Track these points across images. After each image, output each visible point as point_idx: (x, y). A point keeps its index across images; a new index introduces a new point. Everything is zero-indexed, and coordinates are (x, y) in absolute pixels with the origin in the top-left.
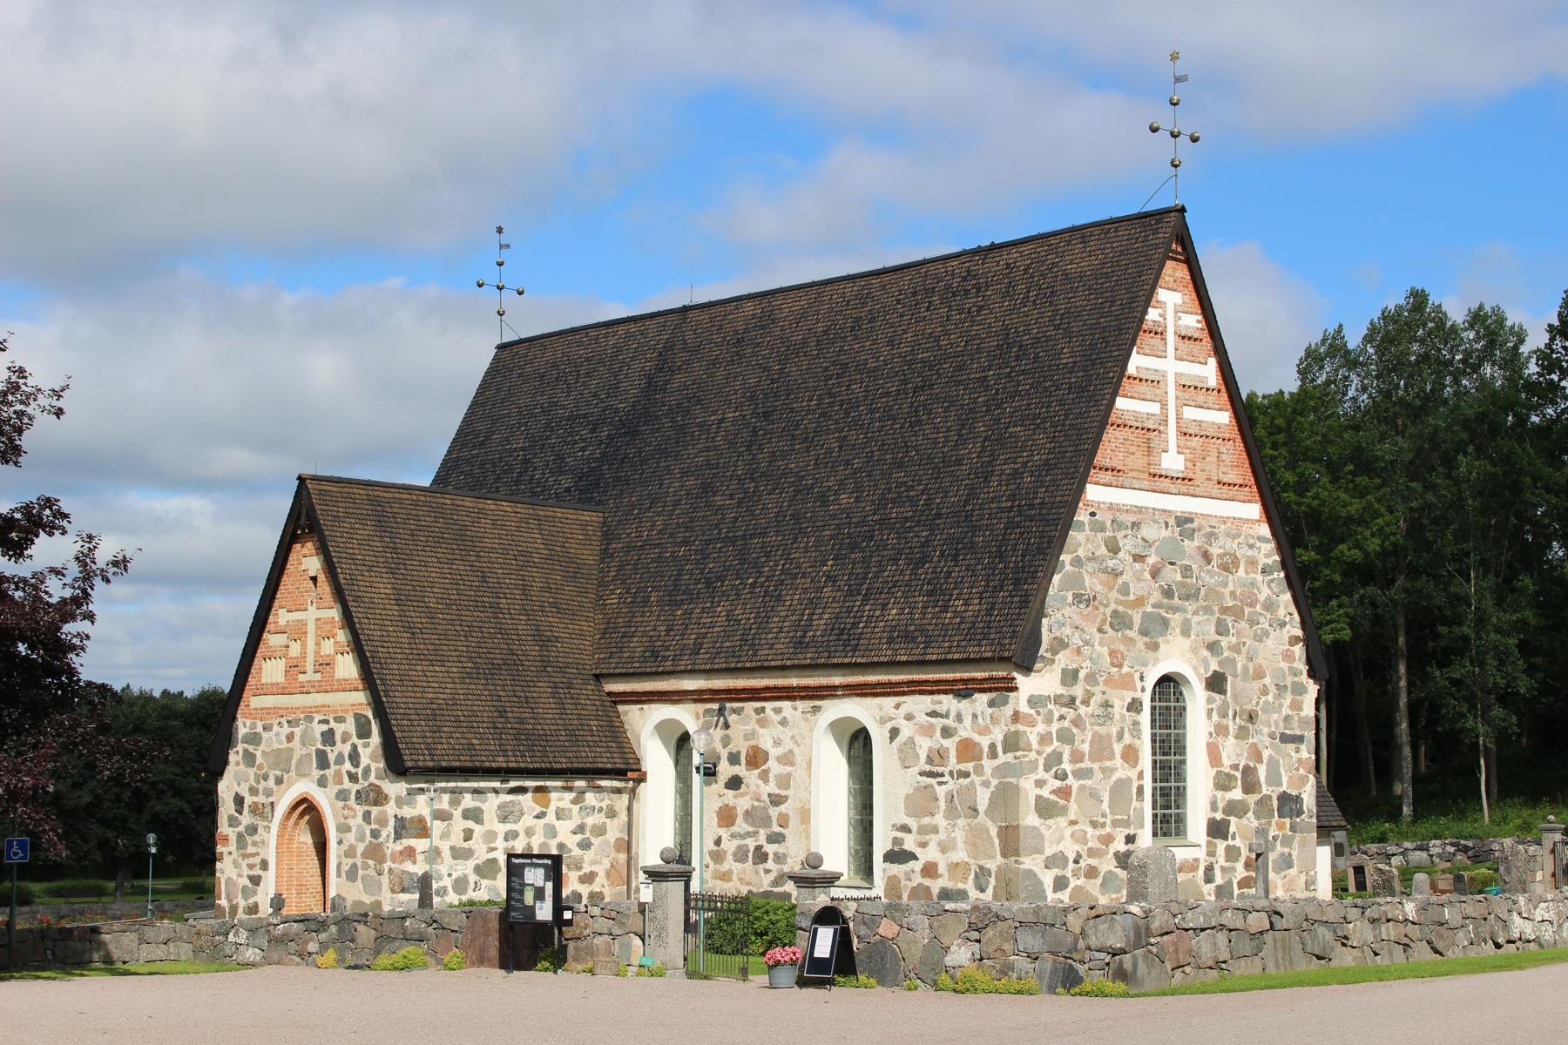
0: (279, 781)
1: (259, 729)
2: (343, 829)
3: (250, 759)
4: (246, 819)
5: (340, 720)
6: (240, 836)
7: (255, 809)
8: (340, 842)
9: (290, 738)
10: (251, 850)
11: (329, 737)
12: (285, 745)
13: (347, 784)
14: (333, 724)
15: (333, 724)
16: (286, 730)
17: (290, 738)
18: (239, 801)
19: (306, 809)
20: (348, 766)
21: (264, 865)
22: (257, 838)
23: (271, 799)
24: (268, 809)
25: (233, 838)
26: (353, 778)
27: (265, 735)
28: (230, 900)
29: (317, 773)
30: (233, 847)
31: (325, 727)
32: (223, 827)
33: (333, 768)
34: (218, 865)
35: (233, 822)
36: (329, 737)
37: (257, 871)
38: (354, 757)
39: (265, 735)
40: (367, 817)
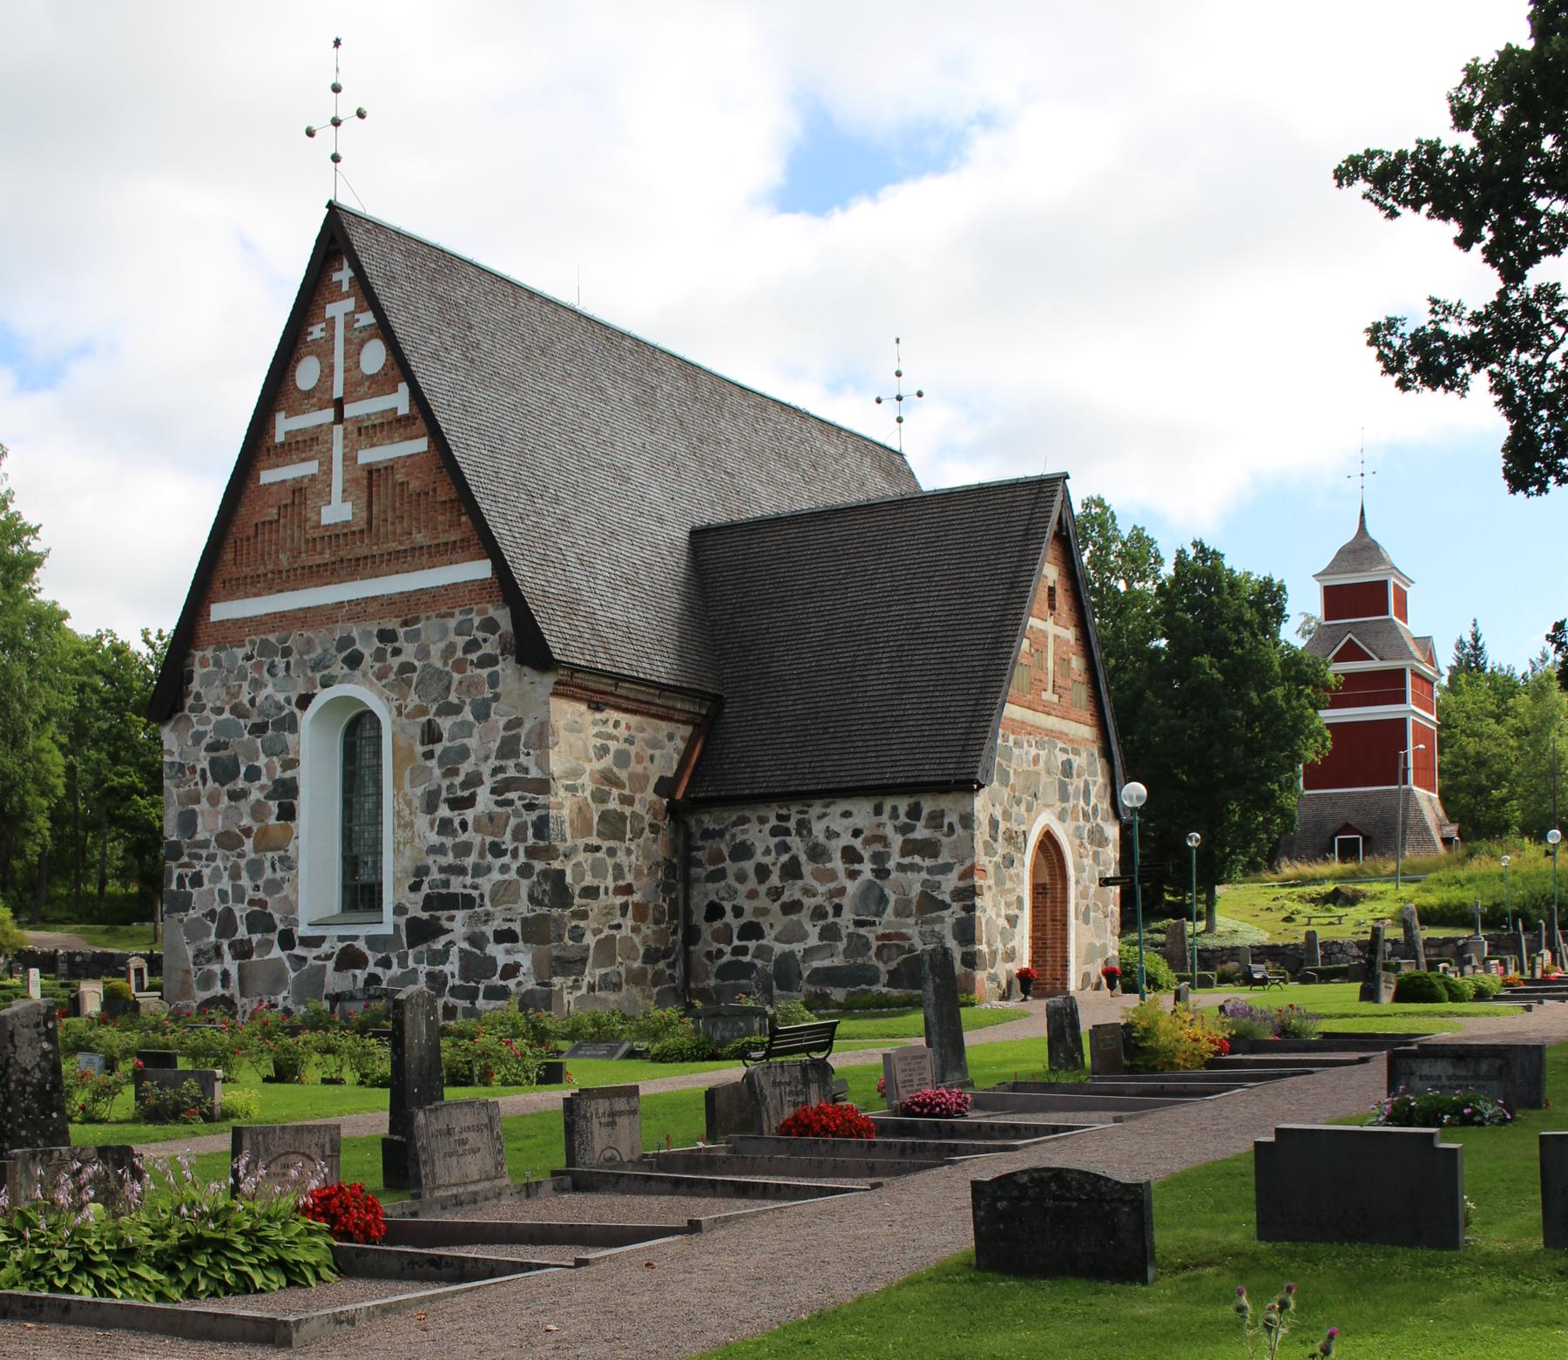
0: (1029, 809)
1: (1011, 743)
2: (1080, 869)
3: (1005, 780)
4: (1001, 848)
5: (1076, 752)
6: (997, 866)
7: (1010, 838)
8: (1077, 882)
9: (1036, 760)
10: (1008, 885)
11: (1067, 768)
12: (1032, 768)
13: (1081, 822)
14: (1071, 756)
15: (1071, 756)
16: (1033, 751)
17: (1036, 760)
18: (994, 824)
19: (1049, 844)
20: (1082, 803)
21: (1020, 901)
22: (1012, 871)
23: (1023, 828)
24: (1021, 839)
25: (990, 869)
26: (1085, 815)
27: (1016, 751)
28: (989, 944)
29: (1059, 806)
30: (991, 882)
31: (1065, 757)
32: (981, 859)
33: (1072, 802)
34: (978, 901)
35: (989, 849)
36: (1067, 768)
37: (1013, 911)
38: (1087, 794)
39: (1016, 751)
40: (1096, 856)
